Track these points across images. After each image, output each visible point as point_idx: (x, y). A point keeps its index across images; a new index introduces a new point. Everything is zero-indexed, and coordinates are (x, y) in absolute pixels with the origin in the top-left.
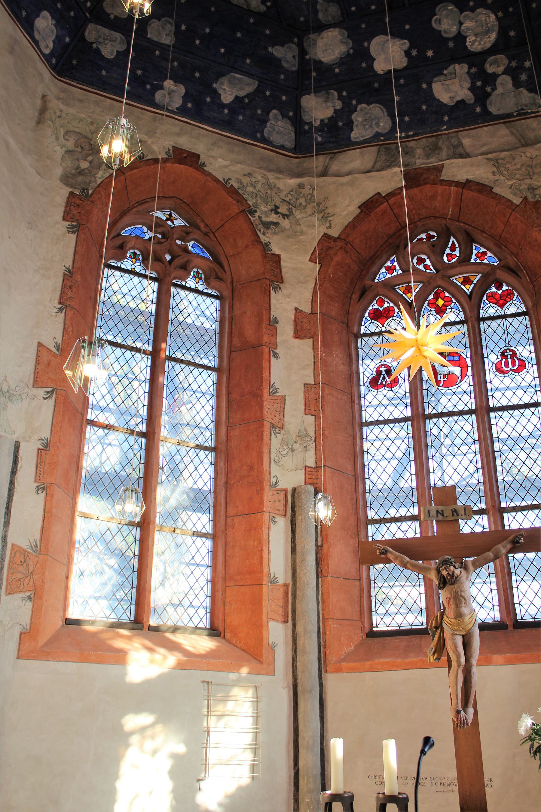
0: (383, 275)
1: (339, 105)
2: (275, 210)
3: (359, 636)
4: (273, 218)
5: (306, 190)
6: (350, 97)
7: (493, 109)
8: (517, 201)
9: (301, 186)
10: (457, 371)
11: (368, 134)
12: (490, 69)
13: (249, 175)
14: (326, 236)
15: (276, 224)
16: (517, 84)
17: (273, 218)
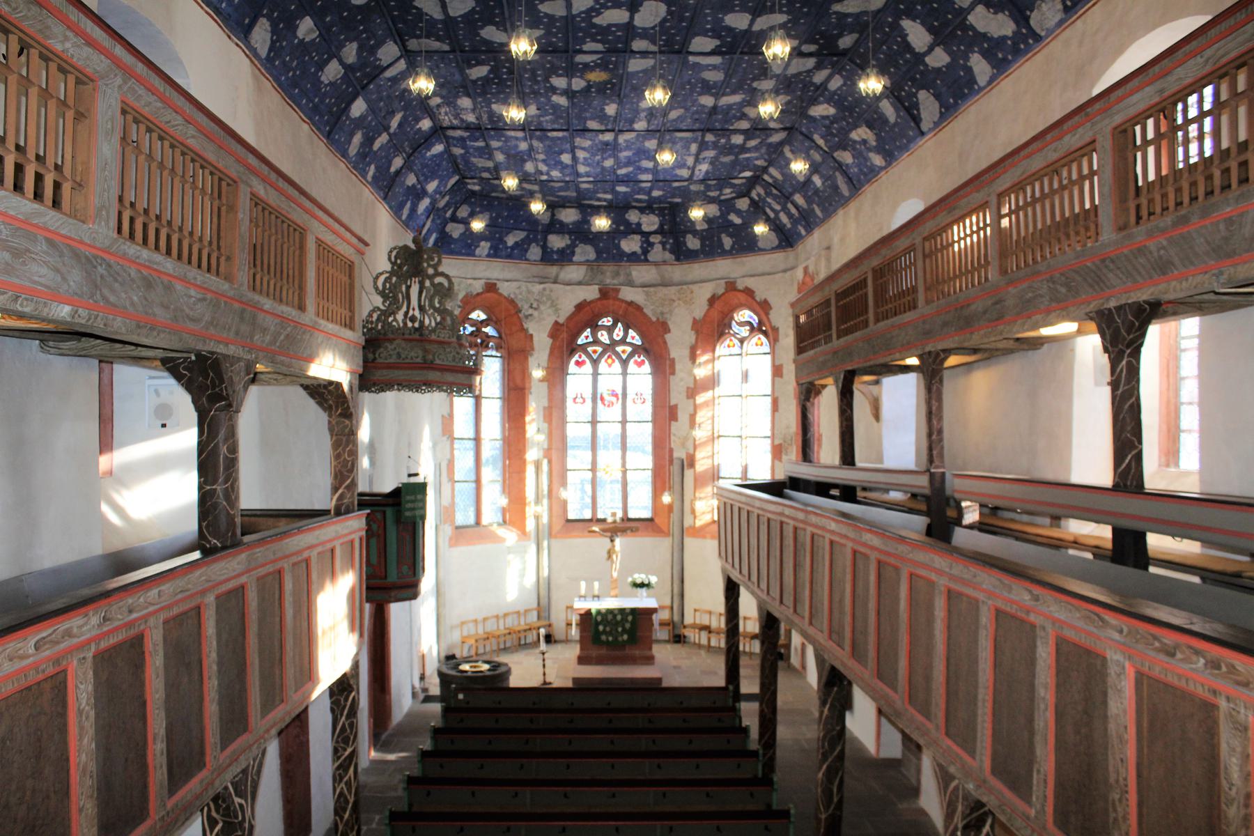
0: (581, 340)
1: (569, 242)
2: (531, 307)
3: (563, 522)
4: (530, 311)
5: (547, 292)
6: (576, 239)
7: (650, 258)
8: (654, 319)
9: (544, 289)
10: (614, 399)
11: (583, 259)
12: (652, 239)
13: (519, 288)
14: (556, 323)
15: (531, 315)
16: (664, 249)
17: (530, 311)
